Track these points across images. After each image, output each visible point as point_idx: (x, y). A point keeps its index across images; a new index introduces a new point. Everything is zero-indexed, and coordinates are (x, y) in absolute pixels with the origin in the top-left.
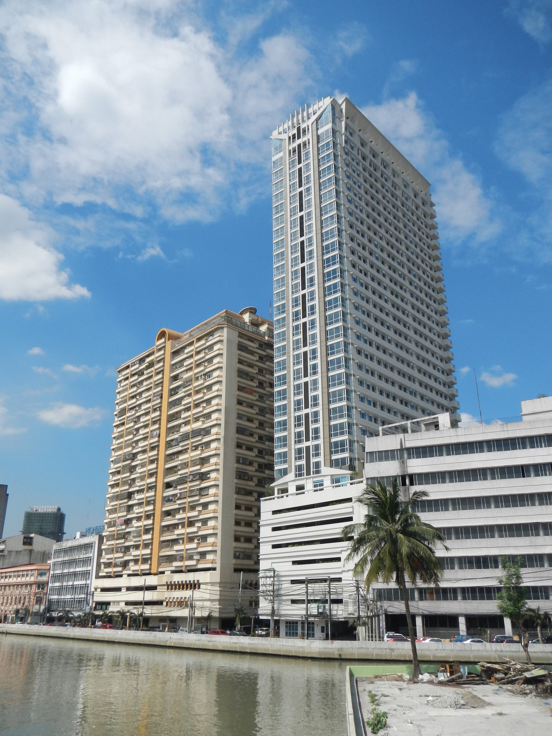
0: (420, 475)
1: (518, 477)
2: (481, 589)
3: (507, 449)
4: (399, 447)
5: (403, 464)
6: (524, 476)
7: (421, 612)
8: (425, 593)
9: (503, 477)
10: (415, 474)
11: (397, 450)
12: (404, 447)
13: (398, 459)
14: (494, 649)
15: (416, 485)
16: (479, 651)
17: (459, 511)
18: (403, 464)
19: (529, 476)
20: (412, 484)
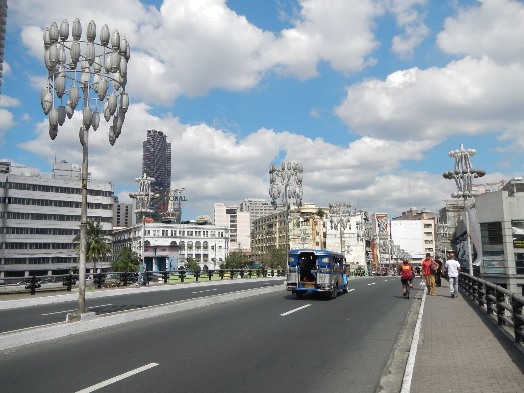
0: (16, 199)
1: (67, 206)
2: (40, 258)
3: (65, 192)
4: (5, 181)
5: (6, 191)
6: (70, 207)
7: (5, 270)
8: (9, 260)
9: (60, 206)
10: (13, 198)
11: (3, 182)
12: (8, 182)
13: (3, 188)
14: (58, 284)
15: (12, 203)
16: (51, 285)
17: (35, 220)
18: (6, 191)
19: (73, 207)
20: (9, 202)
